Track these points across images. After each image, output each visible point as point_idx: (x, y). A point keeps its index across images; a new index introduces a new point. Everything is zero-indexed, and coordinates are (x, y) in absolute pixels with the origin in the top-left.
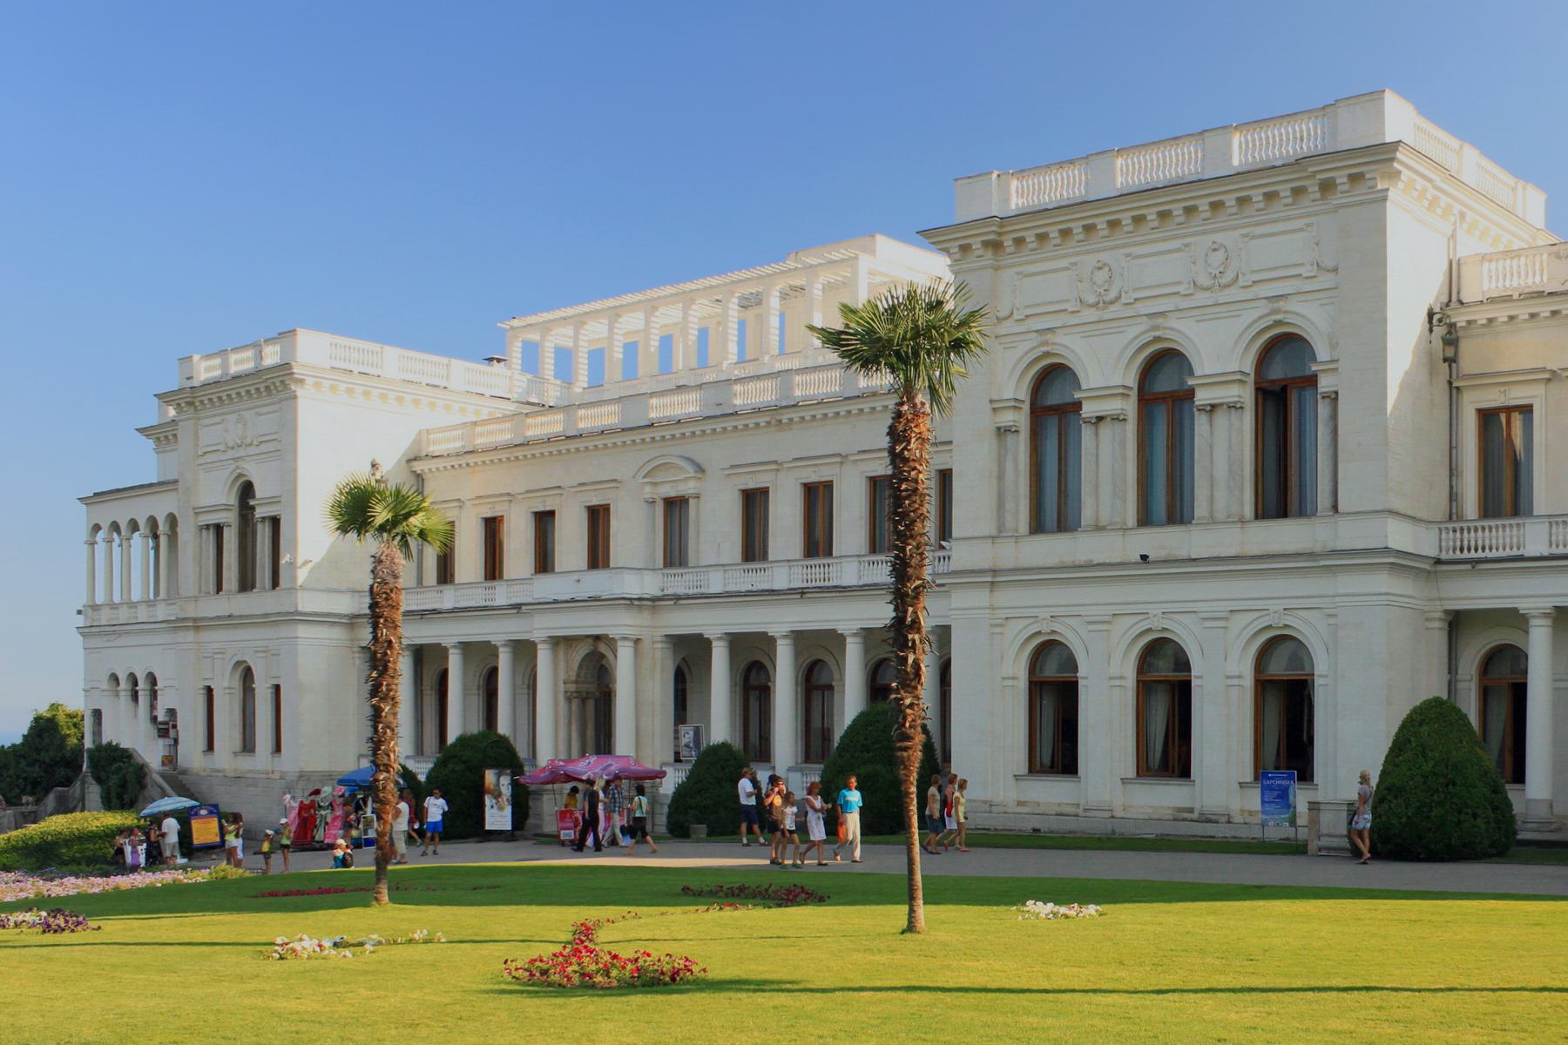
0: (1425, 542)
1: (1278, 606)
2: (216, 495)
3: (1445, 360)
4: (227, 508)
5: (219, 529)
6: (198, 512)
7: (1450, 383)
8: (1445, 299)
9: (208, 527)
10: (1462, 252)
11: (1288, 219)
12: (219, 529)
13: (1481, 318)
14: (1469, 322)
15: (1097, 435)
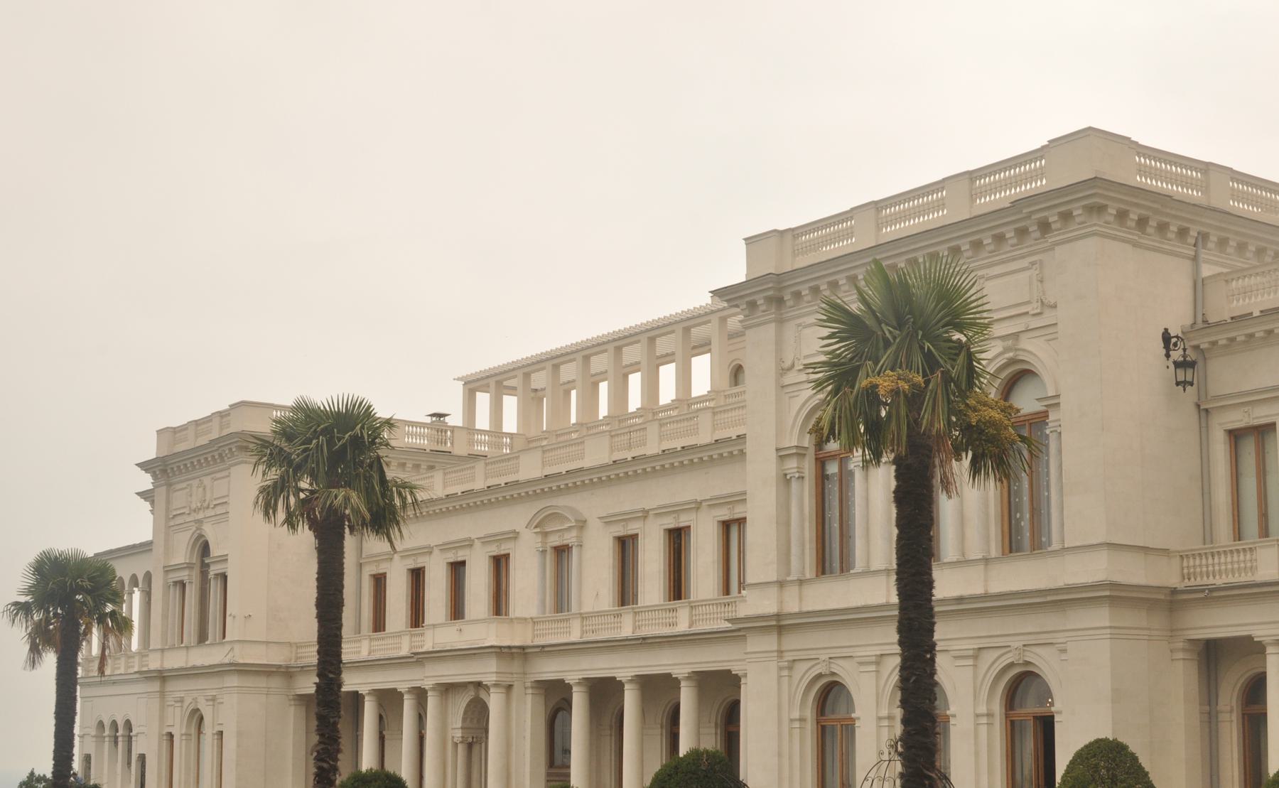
0: (1168, 575)
1: (1016, 643)
2: (182, 553)
3: (1178, 384)
4: (189, 566)
5: (182, 585)
6: (168, 570)
7: (1198, 406)
8: (1189, 321)
9: (175, 583)
10: (1207, 271)
11: (1014, 259)
12: (182, 585)
13: (1222, 339)
14: (1214, 343)
15: (866, 478)
